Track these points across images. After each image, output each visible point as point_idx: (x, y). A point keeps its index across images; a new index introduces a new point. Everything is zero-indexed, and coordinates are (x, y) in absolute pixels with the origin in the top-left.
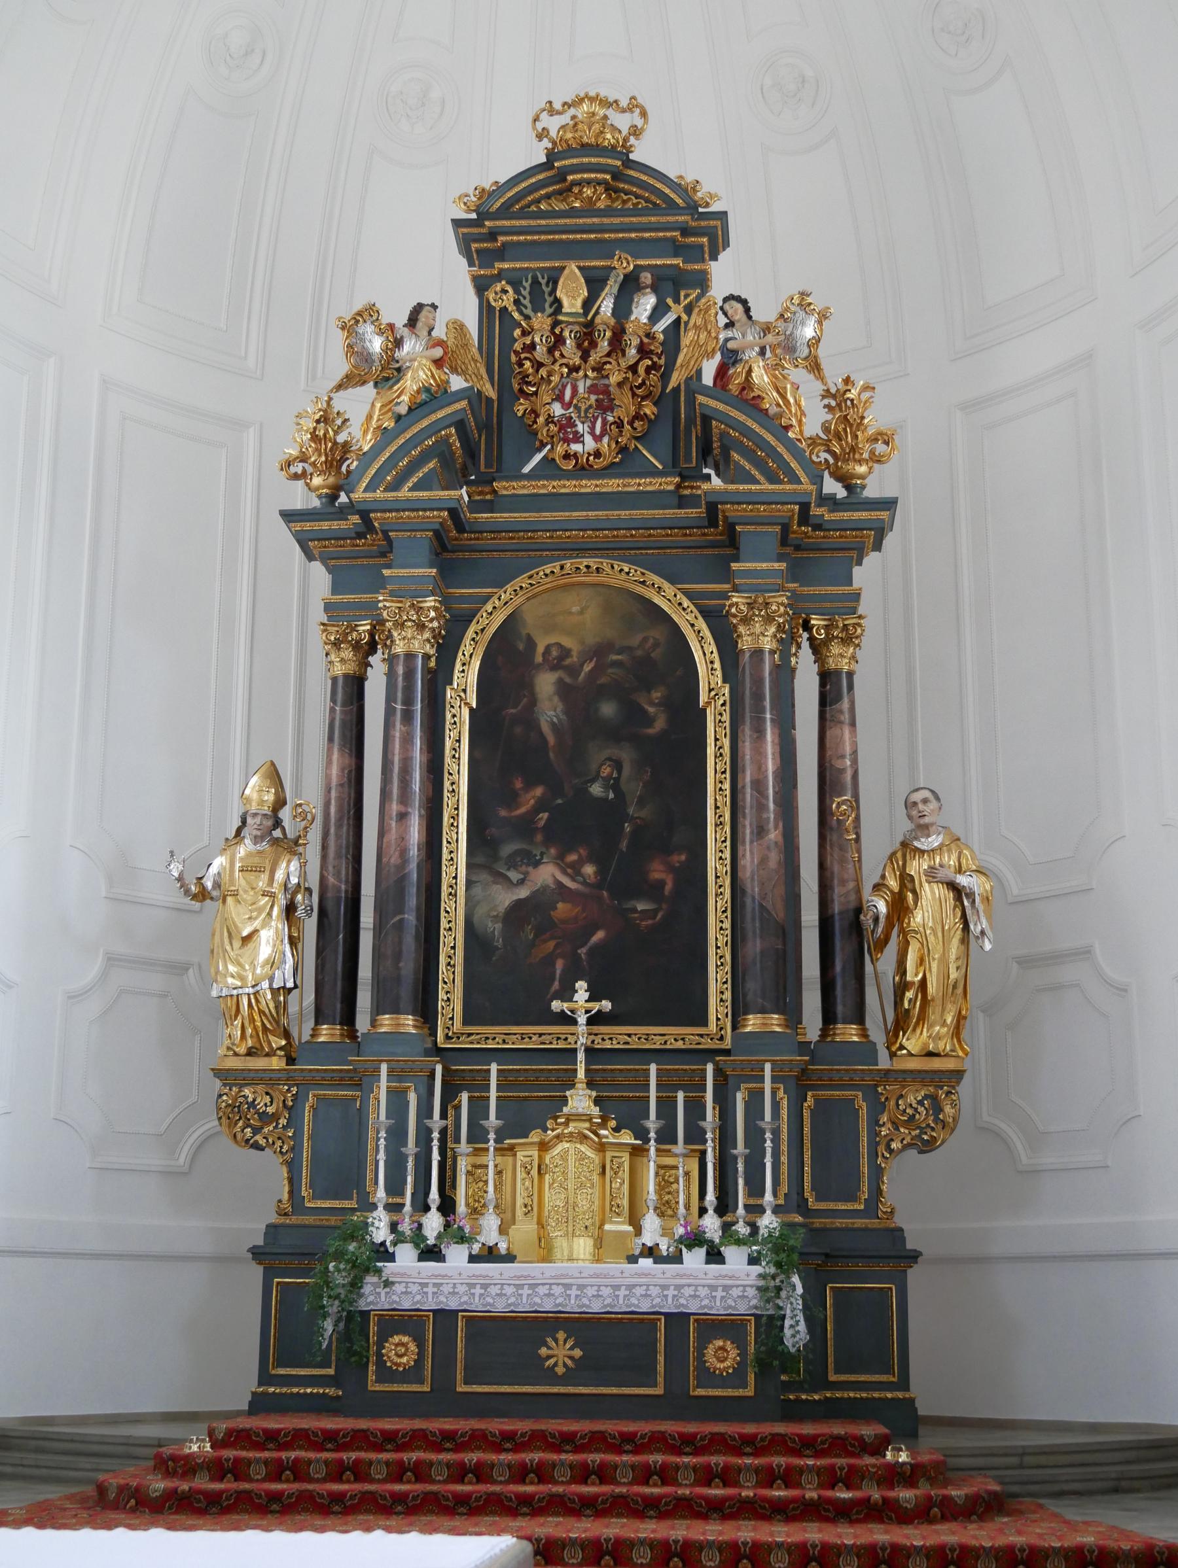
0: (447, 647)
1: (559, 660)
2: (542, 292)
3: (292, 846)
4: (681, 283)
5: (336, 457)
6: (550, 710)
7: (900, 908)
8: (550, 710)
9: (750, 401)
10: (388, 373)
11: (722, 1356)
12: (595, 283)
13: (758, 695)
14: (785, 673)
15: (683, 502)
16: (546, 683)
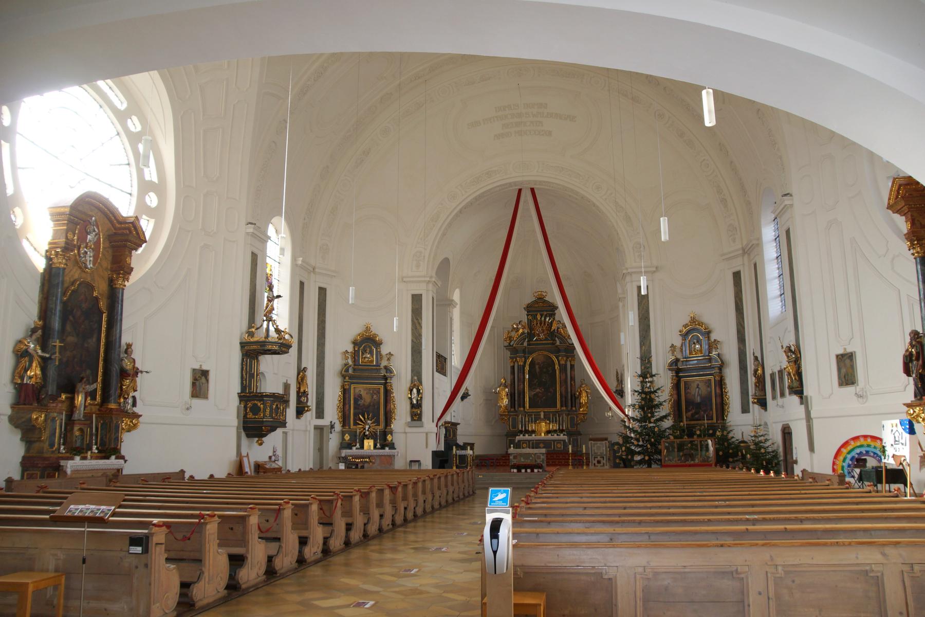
0: (525, 362)
1: (538, 364)
2: (535, 317)
3: (506, 387)
4: (552, 315)
5: (510, 338)
6: (538, 370)
7: (580, 394)
8: (538, 370)
9: (560, 334)
10: (517, 330)
11: (559, 446)
12: (542, 316)
13: (563, 369)
14: (566, 365)
15: (553, 344)
16: (537, 367)
